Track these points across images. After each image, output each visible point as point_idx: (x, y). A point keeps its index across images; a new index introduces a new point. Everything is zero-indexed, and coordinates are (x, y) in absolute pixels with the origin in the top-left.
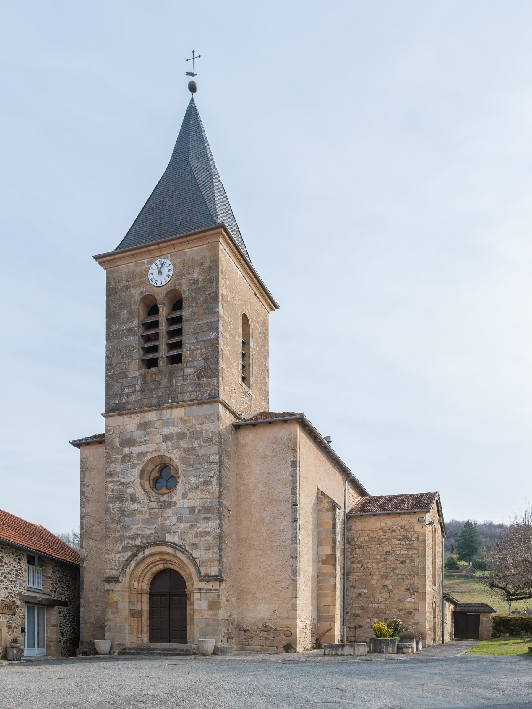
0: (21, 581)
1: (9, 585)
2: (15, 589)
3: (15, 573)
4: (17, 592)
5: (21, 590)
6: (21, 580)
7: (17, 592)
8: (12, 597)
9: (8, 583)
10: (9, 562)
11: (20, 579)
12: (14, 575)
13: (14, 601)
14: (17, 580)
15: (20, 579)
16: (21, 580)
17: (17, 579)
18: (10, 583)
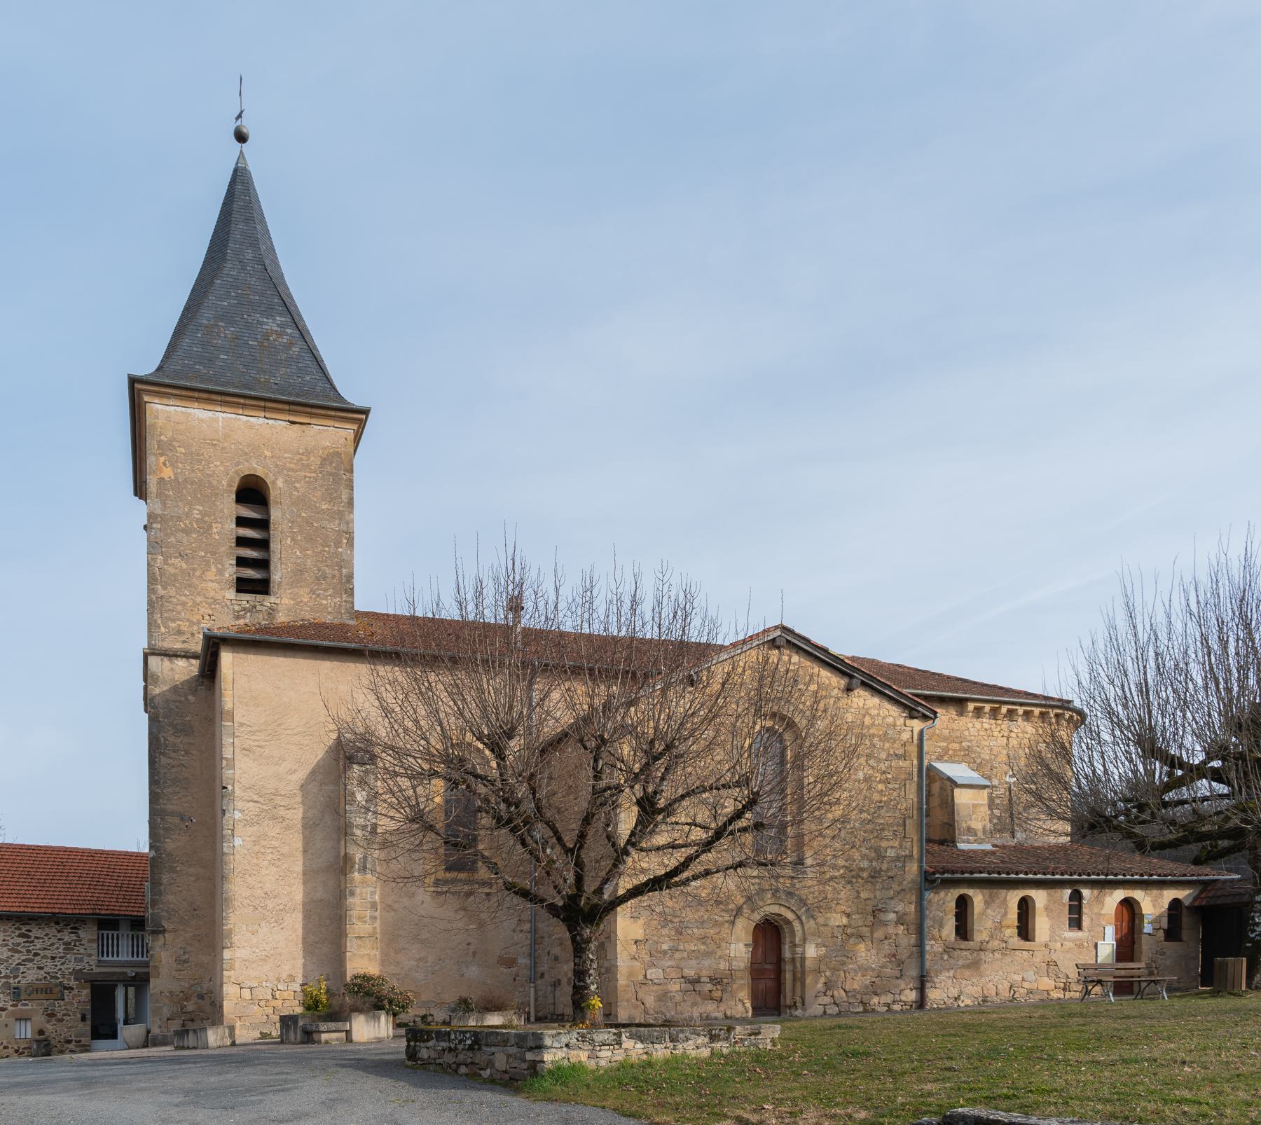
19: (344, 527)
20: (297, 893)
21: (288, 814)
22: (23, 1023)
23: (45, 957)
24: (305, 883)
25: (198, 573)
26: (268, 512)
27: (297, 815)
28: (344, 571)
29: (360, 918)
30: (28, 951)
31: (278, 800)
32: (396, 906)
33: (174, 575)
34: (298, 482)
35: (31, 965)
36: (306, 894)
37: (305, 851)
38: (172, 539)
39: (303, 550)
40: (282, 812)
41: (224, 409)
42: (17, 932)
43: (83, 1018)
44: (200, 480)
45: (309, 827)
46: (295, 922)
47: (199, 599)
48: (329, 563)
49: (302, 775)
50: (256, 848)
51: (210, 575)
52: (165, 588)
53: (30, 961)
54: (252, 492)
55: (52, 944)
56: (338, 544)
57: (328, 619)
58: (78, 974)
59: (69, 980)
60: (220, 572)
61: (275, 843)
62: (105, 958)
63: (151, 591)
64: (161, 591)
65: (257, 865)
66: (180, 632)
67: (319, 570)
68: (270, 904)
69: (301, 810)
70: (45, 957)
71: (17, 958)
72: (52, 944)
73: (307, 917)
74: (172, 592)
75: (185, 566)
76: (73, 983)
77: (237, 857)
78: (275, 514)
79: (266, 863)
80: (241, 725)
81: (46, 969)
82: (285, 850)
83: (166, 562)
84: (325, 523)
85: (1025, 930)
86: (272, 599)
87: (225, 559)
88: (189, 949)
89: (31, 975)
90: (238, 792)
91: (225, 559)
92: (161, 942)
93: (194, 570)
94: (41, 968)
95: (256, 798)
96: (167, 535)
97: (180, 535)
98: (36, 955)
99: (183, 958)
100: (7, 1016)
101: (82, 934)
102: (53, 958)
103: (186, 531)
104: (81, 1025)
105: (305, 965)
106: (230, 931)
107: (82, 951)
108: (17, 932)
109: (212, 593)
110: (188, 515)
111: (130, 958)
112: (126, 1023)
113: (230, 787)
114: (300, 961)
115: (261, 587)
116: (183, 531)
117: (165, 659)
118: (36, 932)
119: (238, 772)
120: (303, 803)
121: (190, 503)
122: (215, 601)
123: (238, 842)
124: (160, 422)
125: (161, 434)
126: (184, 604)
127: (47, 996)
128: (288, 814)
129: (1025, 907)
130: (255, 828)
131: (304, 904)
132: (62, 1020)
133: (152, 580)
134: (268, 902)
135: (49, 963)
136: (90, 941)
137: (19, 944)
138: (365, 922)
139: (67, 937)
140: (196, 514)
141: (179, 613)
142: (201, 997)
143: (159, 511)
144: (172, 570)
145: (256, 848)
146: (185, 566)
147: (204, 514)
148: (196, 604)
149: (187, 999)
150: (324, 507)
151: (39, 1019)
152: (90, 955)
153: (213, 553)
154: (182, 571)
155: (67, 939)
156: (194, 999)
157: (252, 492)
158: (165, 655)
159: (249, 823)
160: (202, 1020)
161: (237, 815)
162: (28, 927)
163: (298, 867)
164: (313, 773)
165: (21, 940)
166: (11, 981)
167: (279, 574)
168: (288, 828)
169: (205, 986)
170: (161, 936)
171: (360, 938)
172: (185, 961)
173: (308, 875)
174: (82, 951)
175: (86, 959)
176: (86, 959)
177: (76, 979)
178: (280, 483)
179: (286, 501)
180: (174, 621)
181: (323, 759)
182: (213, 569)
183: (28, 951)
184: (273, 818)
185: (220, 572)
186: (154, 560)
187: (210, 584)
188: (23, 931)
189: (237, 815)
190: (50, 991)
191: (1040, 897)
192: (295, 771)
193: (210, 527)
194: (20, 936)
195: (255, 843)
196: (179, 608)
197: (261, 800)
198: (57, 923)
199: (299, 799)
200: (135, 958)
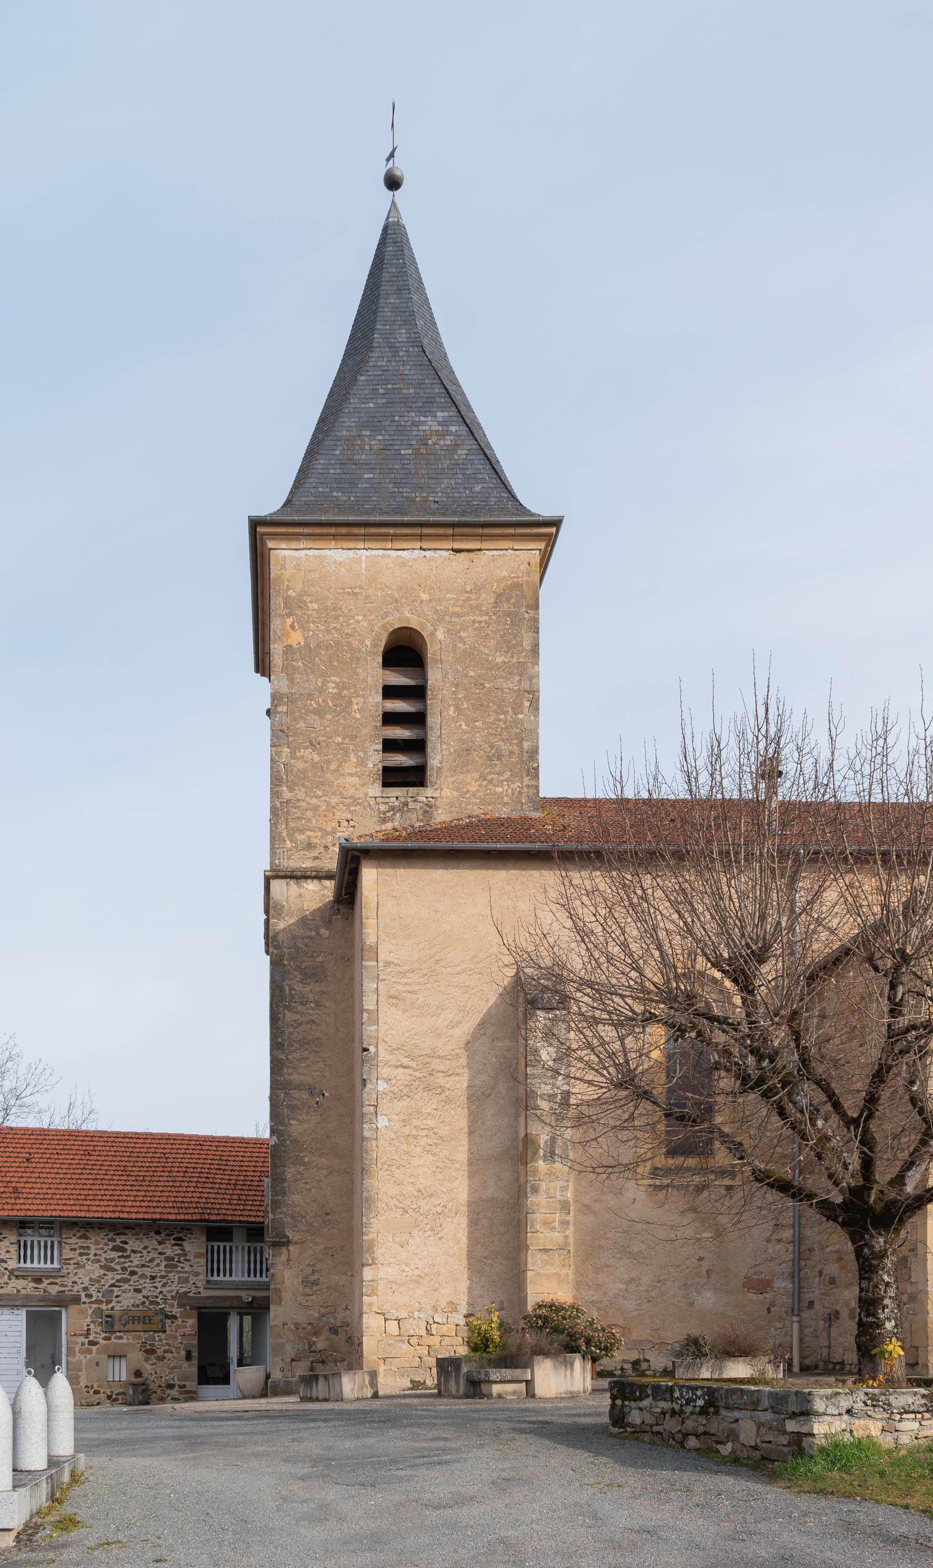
0: (184, 1275)
1: (146, 1285)
2: (164, 1289)
3: (164, 1263)
4: (174, 1294)
5: (182, 1290)
6: (186, 1272)
7: (174, 1294)
8: (158, 1304)
9: (142, 1281)
10: (145, 1248)
11: (179, 1272)
12: (162, 1268)
13: (162, 1309)
14: (171, 1275)
15: (179, 1272)
16: (186, 1272)
17: (170, 1272)
18: (148, 1281)
19: (526, 685)
20: (460, 1190)
21: (449, 1083)
22: (117, 1361)
23: (143, 1276)
24: (470, 1176)
25: (333, 766)
26: (424, 677)
27: (460, 1084)
28: (526, 745)
29: (546, 1223)
30: (124, 1269)
31: (436, 1064)
32: (597, 1207)
33: (304, 772)
34: (464, 629)
35: (126, 1286)
36: (472, 1191)
37: (471, 1133)
38: (301, 725)
39: (471, 721)
40: (440, 1080)
41: (368, 545)
42: (111, 1245)
43: (189, 1357)
44: (337, 643)
45: (477, 1099)
46: (457, 1229)
47: (334, 800)
48: (505, 735)
49: (467, 1027)
50: (406, 1130)
52: (291, 790)
53: (126, 1281)
54: (404, 650)
55: (152, 1260)
56: (517, 709)
57: (504, 812)
58: (182, 1299)
59: (172, 1306)
60: (362, 762)
61: (431, 1123)
62: (215, 1278)
64: (286, 794)
65: (407, 1153)
66: (310, 846)
67: (492, 747)
68: (425, 1205)
69: (466, 1076)
70: (143, 1276)
71: (111, 1278)
72: (152, 1260)
73: (473, 1223)
74: (301, 794)
75: (316, 758)
76: (176, 1311)
77: (381, 1142)
78: (434, 676)
79: (419, 1149)
80: (388, 964)
81: (144, 1292)
82: (445, 1131)
83: (293, 756)
84: (500, 682)
87: (367, 744)
88: (319, 1266)
89: (127, 1300)
90: (383, 1055)
91: (367, 744)
92: (284, 1258)
93: (329, 762)
94: (138, 1291)
95: (406, 1061)
96: (295, 720)
97: (311, 718)
98: (133, 1273)
99: (312, 1278)
100: (98, 1352)
101: (187, 1246)
102: (153, 1278)
104: (185, 1365)
105: (470, 1289)
106: (372, 1243)
107: (187, 1269)
108: (111, 1245)
109: (351, 791)
110: (321, 690)
111: (246, 1278)
112: (240, 1364)
113: (372, 1049)
114: (464, 1284)
115: (414, 777)
116: (315, 712)
117: (292, 882)
118: (133, 1244)
119: (383, 1028)
120: (469, 1066)
121: (324, 675)
122: (355, 801)
123: (382, 1122)
124: (287, 573)
125: (289, 588)
126: (315, 808)
127: (146, 1327)
128: (449, 1083)
130: (404, 1103)
131: (470, 1204)
132: (164, 1358)
133: (276, 781)
134: (422, 1203)
135: (148, 1284)
136: (198, 1256)
137: (113, 1260)
138: (553, 1229)
139: (170, 1250)
140: (332, 689)
141: (310, 821)
142: (334, 1330)
143: (285, 690)
144: (300, 765)
145: (406, 1130)
146: (316, 758)
147: (341, 687)
148: (331, 807)
149: (316, 1334)
150: (499, 660)
151: (136, 1357)
152: (197, 1274)
153: (353, 738)
154: (314, 765)
155: (169, 1252)
156: (325, 1334)
157: (404, 651)
158: (292, 877)
159: (397, 1096)
160: (336, 1362)
161: (382, 1086)
162: (123, 1238)
163: (462, 1155)
164: (482, 1024)
165: (115, 1254)
166: (104, 1307)
167: (439, 757)
168: (448, 1101)
169: (340, 1317)
170: (284, 1249)
171: (546, 1251)
172: (315, 1283)
173: (476, 1165)
174: (187, 1269)
175: (192, 1279)
176: (192, 1279)
177: (180, 1305)
178: (440, 635)
179: (449, 657)
180: (302, 832)
181: (496, 1005)
182: (353, 758)
183: (124, 1269)
184: (428, 1088)
185: (362, 762)
186: (279, 754)
187: (349, 779)
188: (118, 1243)
189: (382, 1086)
190: (149, 1320)
192: (459, 1023)
193: (350, 703)
194: (115, 1249)
195: (405, 1123)
196: (309, 814)
197: (413, 1064)
198: (158, 1233)
199: (463, 1061)
200: (252, 1278)
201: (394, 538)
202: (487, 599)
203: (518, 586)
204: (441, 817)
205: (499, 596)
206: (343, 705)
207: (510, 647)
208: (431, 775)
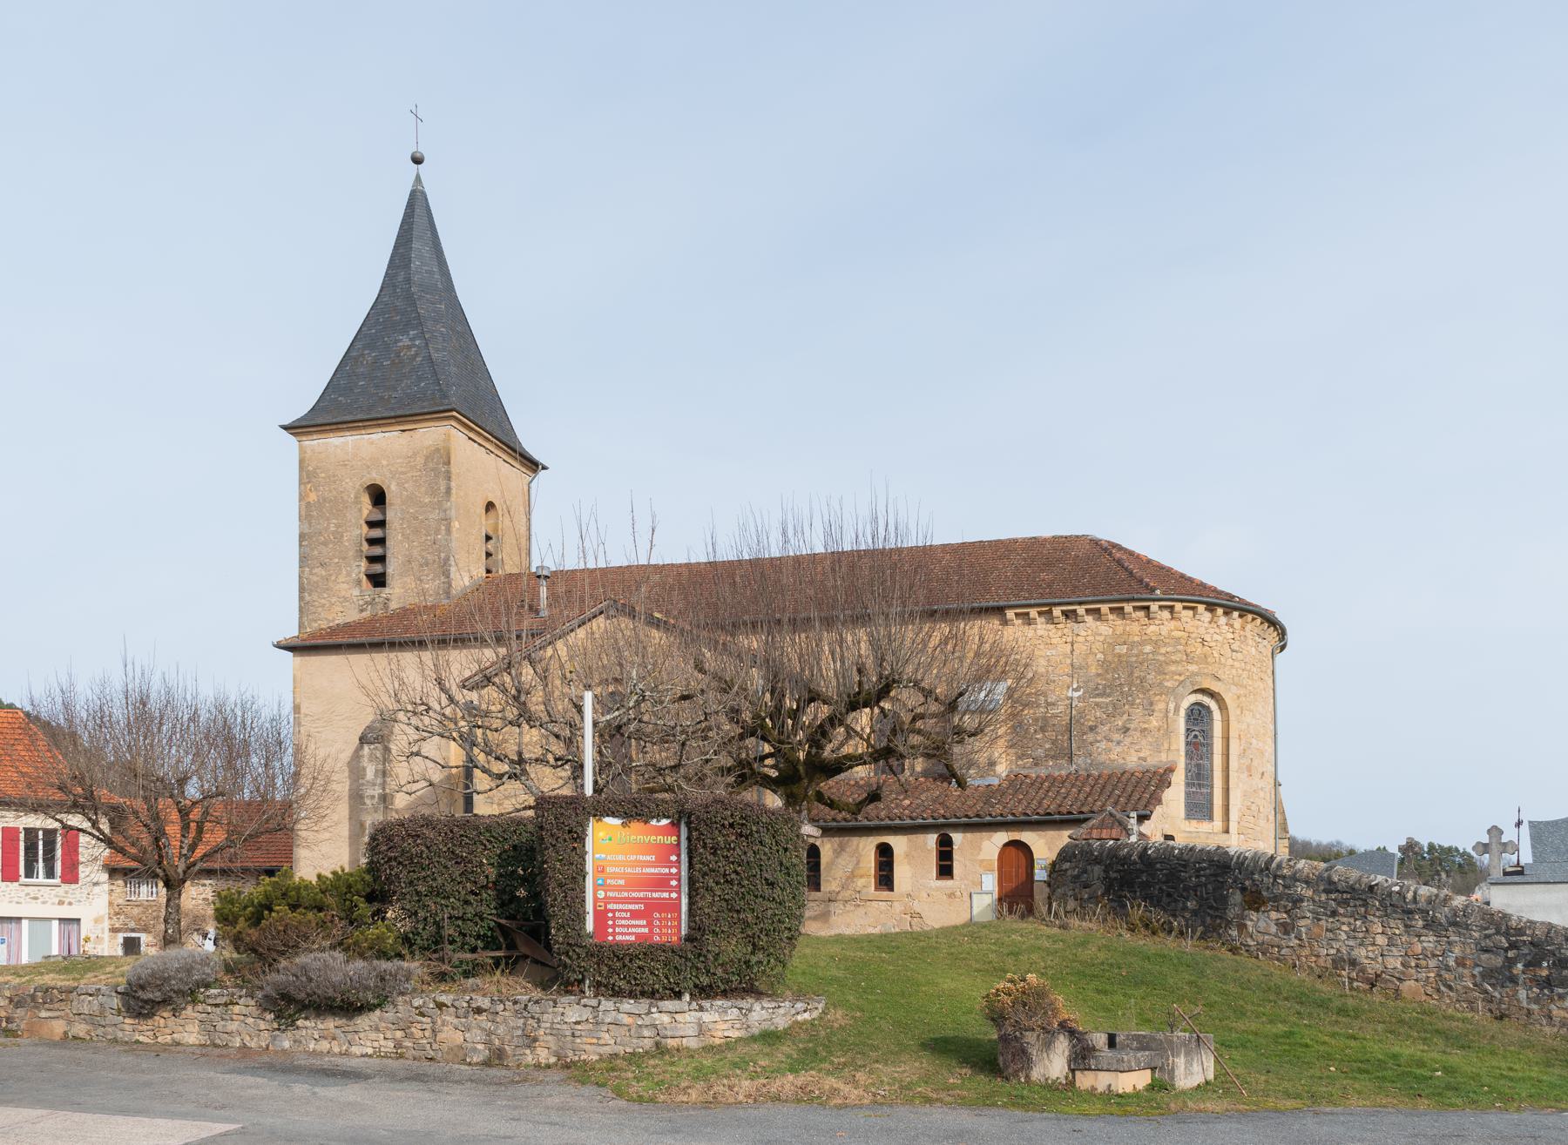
19: (442, 515)
51: (341, 579)
56: (437, 532)
60: (349, 574)
63: (301, 598)
64: (307, 598)
78: (391, 515)
85: (885, 878)
86: (387, 590)
103: (325, 544)
110: (326, 529)
115: (378, 580)
129: (885, 852)
133: (302, 589)
144: (315, 579)
147: (338, 526)
178: (393, 487)
185: (349, 574)
191: (898, 843)
201: (364, 427)
202: (420, 460)
203: (438, 450)
204: (394, 605)
205: (427, 458)
206: (338, 536)
207: (433, 492)
208: (389, 580)
